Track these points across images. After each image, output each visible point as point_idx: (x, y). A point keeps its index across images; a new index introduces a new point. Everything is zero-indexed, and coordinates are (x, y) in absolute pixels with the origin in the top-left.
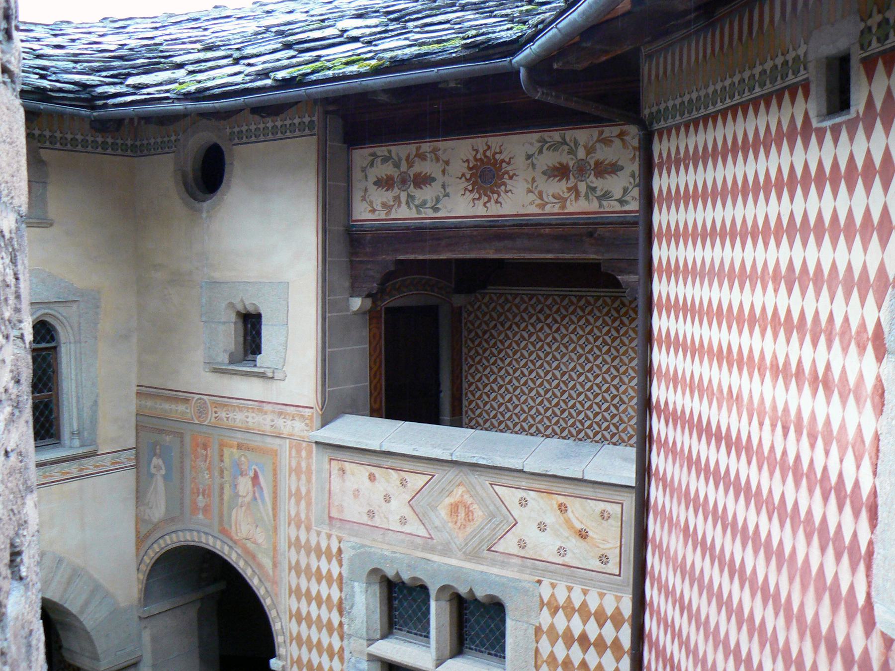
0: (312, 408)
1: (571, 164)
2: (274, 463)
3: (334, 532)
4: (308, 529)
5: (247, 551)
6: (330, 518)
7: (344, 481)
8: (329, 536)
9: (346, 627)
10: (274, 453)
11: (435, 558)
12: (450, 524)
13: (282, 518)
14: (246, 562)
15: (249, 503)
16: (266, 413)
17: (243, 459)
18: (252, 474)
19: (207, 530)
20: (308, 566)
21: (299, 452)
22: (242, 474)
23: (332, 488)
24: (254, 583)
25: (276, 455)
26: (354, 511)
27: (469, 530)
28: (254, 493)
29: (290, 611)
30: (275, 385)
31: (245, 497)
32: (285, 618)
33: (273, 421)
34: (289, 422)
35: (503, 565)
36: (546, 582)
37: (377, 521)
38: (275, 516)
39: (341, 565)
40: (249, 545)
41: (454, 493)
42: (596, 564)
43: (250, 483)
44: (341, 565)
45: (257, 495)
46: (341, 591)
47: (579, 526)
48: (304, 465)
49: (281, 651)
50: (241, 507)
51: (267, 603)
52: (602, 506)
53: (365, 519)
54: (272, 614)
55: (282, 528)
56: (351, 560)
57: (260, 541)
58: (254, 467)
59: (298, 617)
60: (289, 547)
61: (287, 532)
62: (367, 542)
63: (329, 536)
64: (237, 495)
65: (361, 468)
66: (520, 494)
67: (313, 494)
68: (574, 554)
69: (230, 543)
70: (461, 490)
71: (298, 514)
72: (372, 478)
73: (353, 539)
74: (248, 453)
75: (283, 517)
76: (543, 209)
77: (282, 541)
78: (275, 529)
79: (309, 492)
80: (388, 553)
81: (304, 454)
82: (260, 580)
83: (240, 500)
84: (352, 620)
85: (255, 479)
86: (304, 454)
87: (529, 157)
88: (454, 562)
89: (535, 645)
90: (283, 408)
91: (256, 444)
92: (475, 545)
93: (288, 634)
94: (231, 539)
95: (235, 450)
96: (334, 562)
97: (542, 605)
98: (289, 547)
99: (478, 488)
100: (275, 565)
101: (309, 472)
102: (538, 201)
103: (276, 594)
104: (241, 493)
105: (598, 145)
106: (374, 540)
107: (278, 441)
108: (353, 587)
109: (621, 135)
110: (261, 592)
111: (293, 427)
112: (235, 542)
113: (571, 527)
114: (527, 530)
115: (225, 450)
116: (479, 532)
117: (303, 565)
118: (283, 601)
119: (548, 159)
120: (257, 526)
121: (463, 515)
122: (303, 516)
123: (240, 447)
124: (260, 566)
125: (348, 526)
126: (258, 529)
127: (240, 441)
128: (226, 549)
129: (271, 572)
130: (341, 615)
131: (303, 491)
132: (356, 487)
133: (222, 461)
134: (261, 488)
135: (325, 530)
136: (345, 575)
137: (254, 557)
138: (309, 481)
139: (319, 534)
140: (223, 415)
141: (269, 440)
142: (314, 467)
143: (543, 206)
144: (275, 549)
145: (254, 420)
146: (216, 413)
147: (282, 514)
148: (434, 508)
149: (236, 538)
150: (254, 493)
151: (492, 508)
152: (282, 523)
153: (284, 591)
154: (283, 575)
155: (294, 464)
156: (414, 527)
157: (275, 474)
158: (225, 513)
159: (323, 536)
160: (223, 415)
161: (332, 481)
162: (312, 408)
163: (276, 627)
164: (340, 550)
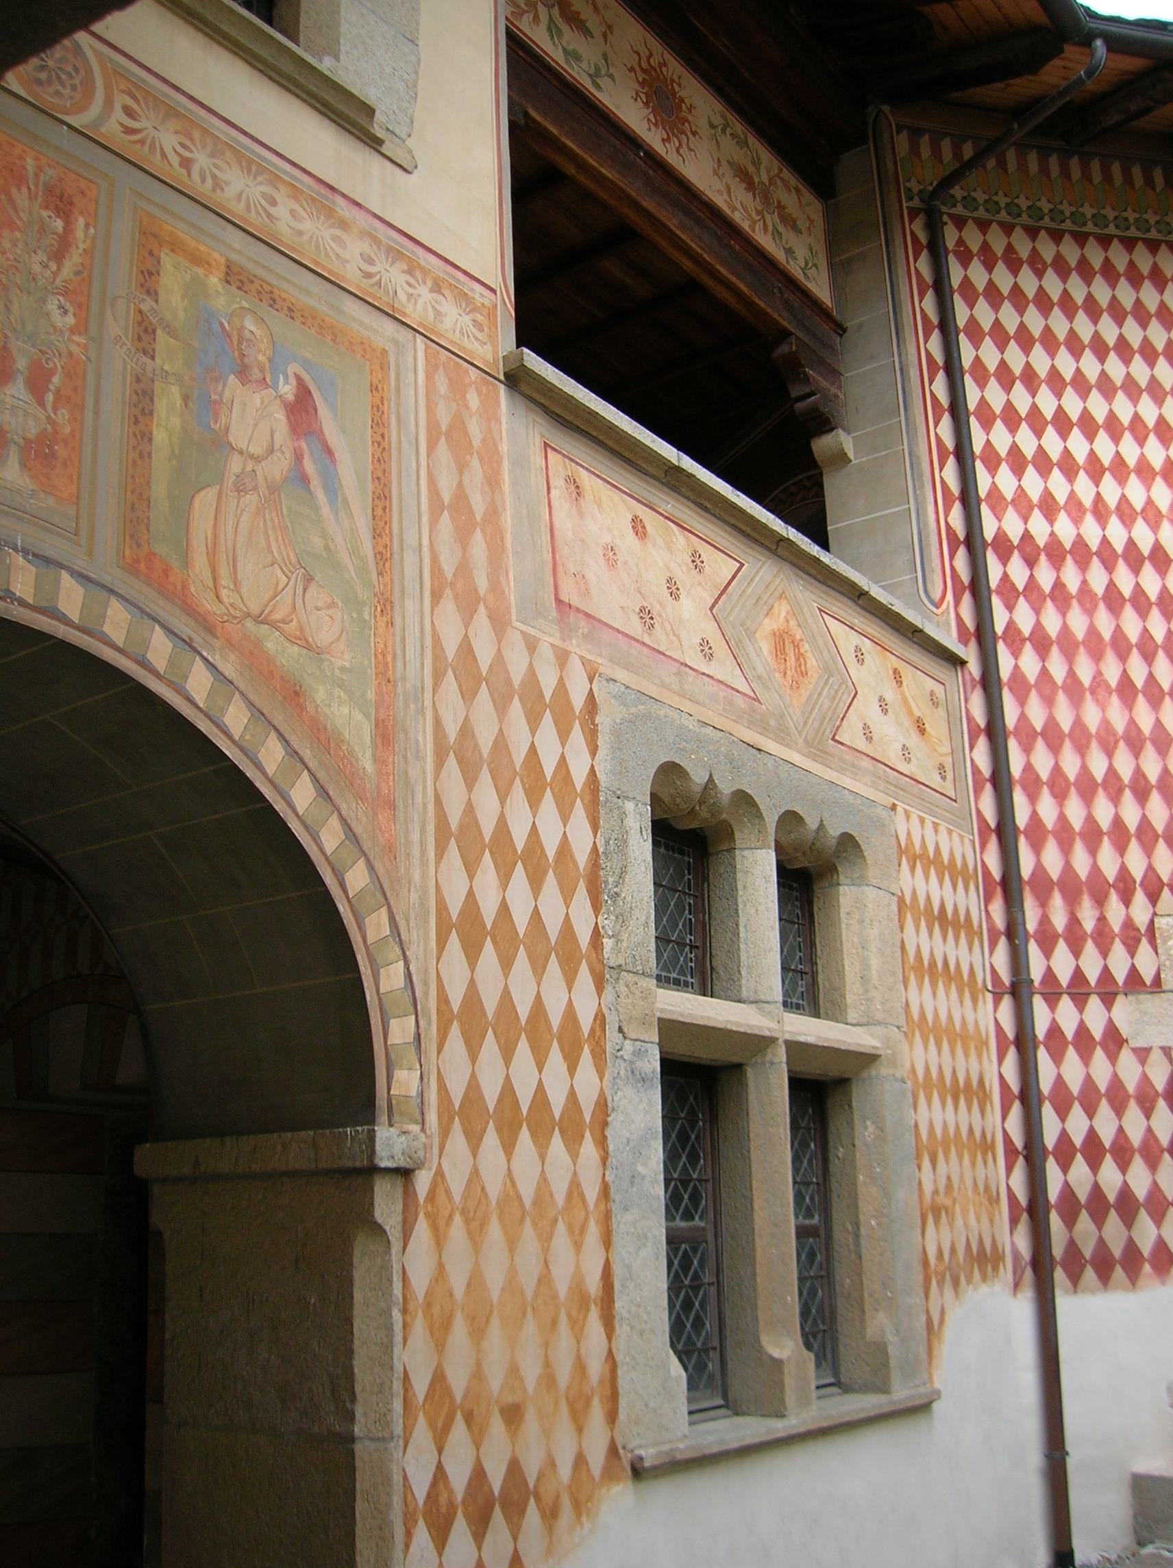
0: (494, 291)
1: (756, 180)
2: (374, 388)
3: (576, 648)
4: (499, 623)
5: (261, 667)
6: (559, 601)
7: (581, 515)
8: (562, 657)
9: (608, 943)
10: (381, 361)
11: (771, 746)
12: (777, 675)
13: (410, 570)
14: (258, 714)
15: (273, 489)
16: (343, 225)
17: (250, 325)
18: (287, 390)
19: (52, 546)
20: (501, 745)
21: (458, 388)
22: (243, 374)
23: (557, 524)
24: (297, 801)
25: (384, 367)
26: (612, 601)
27: (804, 693)
28: (299, 457)
29: (442, 908)
30: (376, 162)
31: (257, 459)
32: (422, 938)
33: (370, 261)
34: (425, 294)
35: (856, 772)
36: (901, 807)
37: (660, 639)
38: (383, 558)
39: (593, 751)
40: (273, 643)
41: (776, 609)
42: (934, 779)
43: (281, 416)
44: (593, 751)
45: (309, 466)
46: (595, 827)
47: (917, 713)
48: (475, 429)
49: (402, 1082)
50: (240, 490)
51: (350, 883)
52: (930, 684)
53: (635, 627)
54: (369, 931)
55: (411, 607)
56: (617, 733)
57: (323, 636)
58: (293, 368)
59: (470, 929)
60: (438, 677)
61: (428, 625)
62: (653, 691)
63: (562, 657)
64: (220, 444)
65: (616, 496)
66: (856, 639)
67: (508, 520)
68: (918, 759)
69: (185, 627)
70: (783, 609)
71: (464, 569)
72: (638, 527)
73: (621, 675)
74: (264, 309)
75: (411, 567)
76: (733, 212)
77: (411, 651)
78: (386, 605)
79: (493, 513)
80: (690, 724)
81: (473, 400)
82: (323, 792)
83: (236, 465)
84: (622, 919)
85: (301, 408)
86: (473, 400)
87: (712, 126)
88: (796, 758)
89: (898, 938)
90: (406, 246)
91: (311, 302)
92: (816, 726)
93: (433, 1004)
94: (190, 610)
95: (214, 280)
96: (577, 736)
97: (901, 851)
98: (438, 677)
99: (805, 610)
100: (385, 735)
101: (491, 458)
102: (725, 196)
103: (391, 849)
104: (239, 436)
105: (779, 182)
106: (663, 685)
107: (389, 327)
108: (622, 816)
109: (797, 189)
110: (324, 841)
111: (438, 314)
112: (209, 628)
113: (910, 713)
114: (866, 707)
115: (167, 260)
116: (818, 699)
117: (485, 739)
118: (417, 877)
119: (729, 147)
120: (309, 579)
121: (793, 660)
122: (482, 583)
123: (234, 276)
124: (324, 737)
125: (606, 636)
126: (313, 590)
127: (233, 256)
128: (160, 649)
129: (369, 766)
130: (596, 906)
131: (478, 505)
132: (607, 538)
133: (153, 294)
134: (330, 452)
135: (549, 638)
136: (601, 777)
137: (294, 695)
138: (493, 481)
139: (531, 646)
140: (168, 140)
141: (353, 308)
142: (504, 448)
143: (734, 209)
144: (385, 677)
145: (289, 219)
146: (128, 112)
147: (410, 560)
148: (751, 635)
149: (208, 605)
150: (299, 457)
151: (826, 654)
152: (412, 587)
153: (417, 833)
154: (414, 773)
155: (444, 417)
156: (723, 668)
157: (379, 423)
158: (159, 491)
159: (545, 652)
160: (168, 140)
161: (555, 503)
162: (494, 291)
163: (384, 980)
164: (591, 703)
